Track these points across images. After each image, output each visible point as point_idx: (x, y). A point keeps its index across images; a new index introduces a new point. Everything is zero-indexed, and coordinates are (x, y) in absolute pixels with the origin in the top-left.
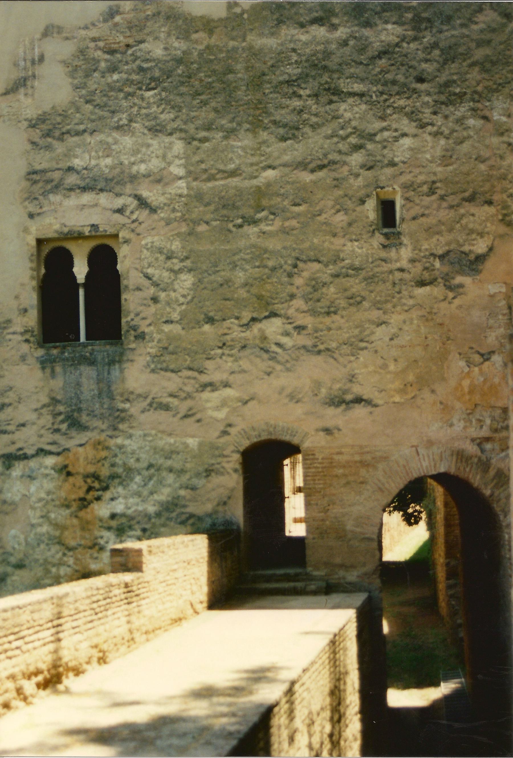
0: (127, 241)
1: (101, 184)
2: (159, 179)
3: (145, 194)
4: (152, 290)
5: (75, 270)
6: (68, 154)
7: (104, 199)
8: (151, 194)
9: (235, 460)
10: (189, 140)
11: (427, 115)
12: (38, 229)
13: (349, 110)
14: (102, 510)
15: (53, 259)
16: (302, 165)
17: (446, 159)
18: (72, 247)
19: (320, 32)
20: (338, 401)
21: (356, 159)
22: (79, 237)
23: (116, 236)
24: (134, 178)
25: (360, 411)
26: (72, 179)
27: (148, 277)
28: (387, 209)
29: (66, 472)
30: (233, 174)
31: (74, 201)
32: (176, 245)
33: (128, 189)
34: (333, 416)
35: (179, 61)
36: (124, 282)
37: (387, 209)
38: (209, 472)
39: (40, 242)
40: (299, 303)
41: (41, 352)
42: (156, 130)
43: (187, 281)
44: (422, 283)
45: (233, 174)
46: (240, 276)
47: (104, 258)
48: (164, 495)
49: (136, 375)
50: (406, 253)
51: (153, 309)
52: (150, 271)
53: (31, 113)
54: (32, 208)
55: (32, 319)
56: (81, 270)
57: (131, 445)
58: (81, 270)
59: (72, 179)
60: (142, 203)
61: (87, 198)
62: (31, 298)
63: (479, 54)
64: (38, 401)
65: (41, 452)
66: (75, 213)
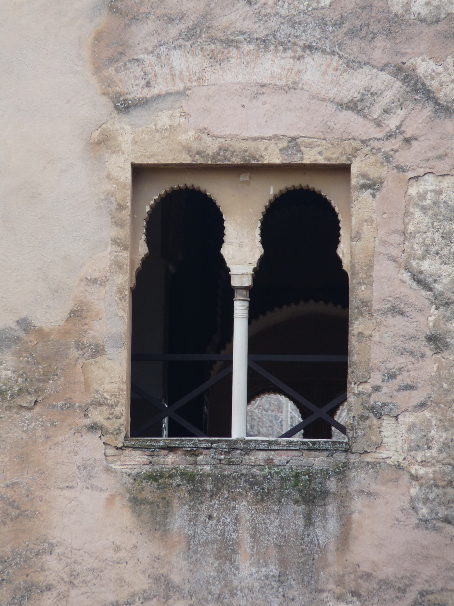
0: (373, 186)
1: (311, 35)
3: (423, 67)
4: (434, 314)
5: (227, 251)
7: (316, 72)
15: (177, 221)
23: (343, 170)
27: (421, 281)
31: (236, 72)
33: (380, 51)
36: (358, 292)
39: (140, 172)
41: (136, 461)
47: (304, 222)
51: (431, 365)
52: (428, 266)
56: (242, 252)
58: (242, 252)
61: (272, 66)
64: (121, 582)
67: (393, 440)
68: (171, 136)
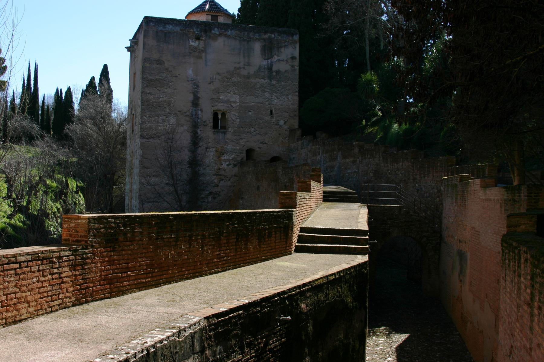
2: (235, 102)
6: (219, 96)
7: (225, 105)
8: (234, 105)
9: (245, 152)
10: (240, 96)
11: (279, 97)
12: (213, 109)
13: (267, 95)
14: (223, 158)
15: (215, 114)
16: (258, 103)
17: (281, 105)
18: (218, 112)
19: (263, 80)
20: (262, 143)
21: (267, 103)
22: (221, 111)
24: (230, 102)
25: (265, 145)
26: (220, 100)
28: (271, 112)
29: (216, 151)
30: (247, 103)
31: (220, 104)
32: (237, 114)
34: (261, 145)
35: (239, 82)
37: (271, 112)
38: (241, 153)
40: (256, 126)
42: (235, 94)
43: (238, 120)
44: (276, 125)
45: (247, 103)
46: (247, 120)
47: (224, 114)
48: (233, 156)
49: (229, 136)
50: (274, 119)
53: (213, 88)
54: (213, 105)
55: (212, 124)
56: (220, 116)
57: (228, 147)
59: (220, 100)
60: (232, 106)
61: (222, 104)
62: (211, 120)
63: (288, 88)
65: (212, 147)
66: (221, 107)
67: (230, 129)
68: (215, 108)
